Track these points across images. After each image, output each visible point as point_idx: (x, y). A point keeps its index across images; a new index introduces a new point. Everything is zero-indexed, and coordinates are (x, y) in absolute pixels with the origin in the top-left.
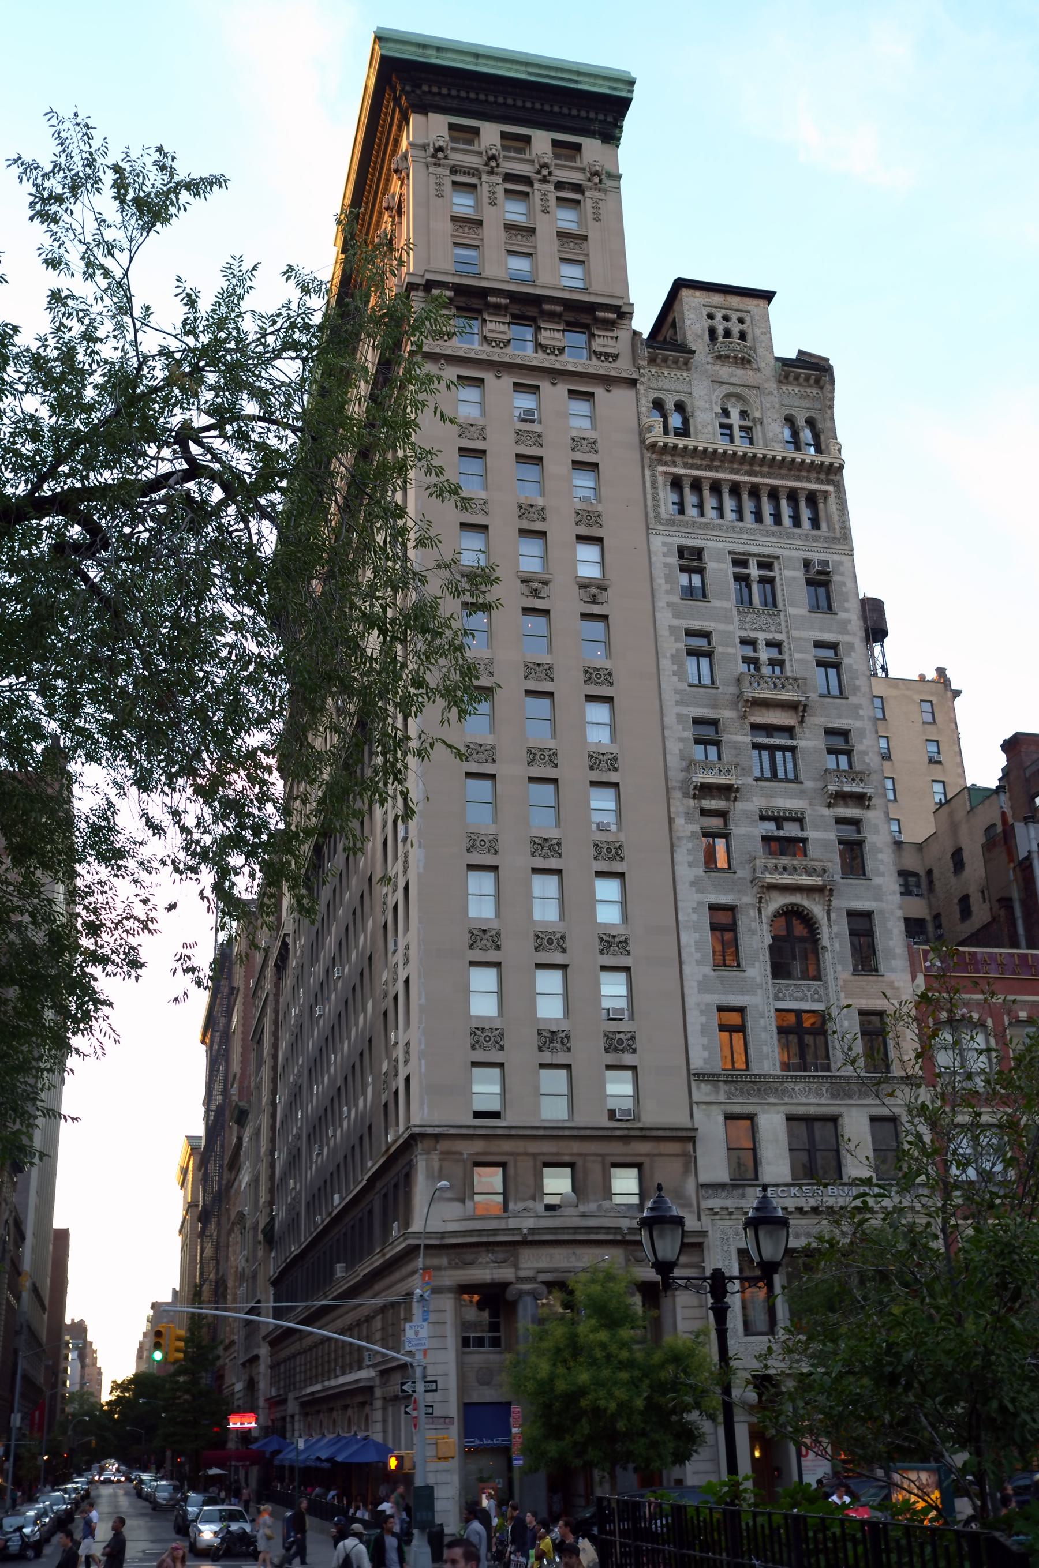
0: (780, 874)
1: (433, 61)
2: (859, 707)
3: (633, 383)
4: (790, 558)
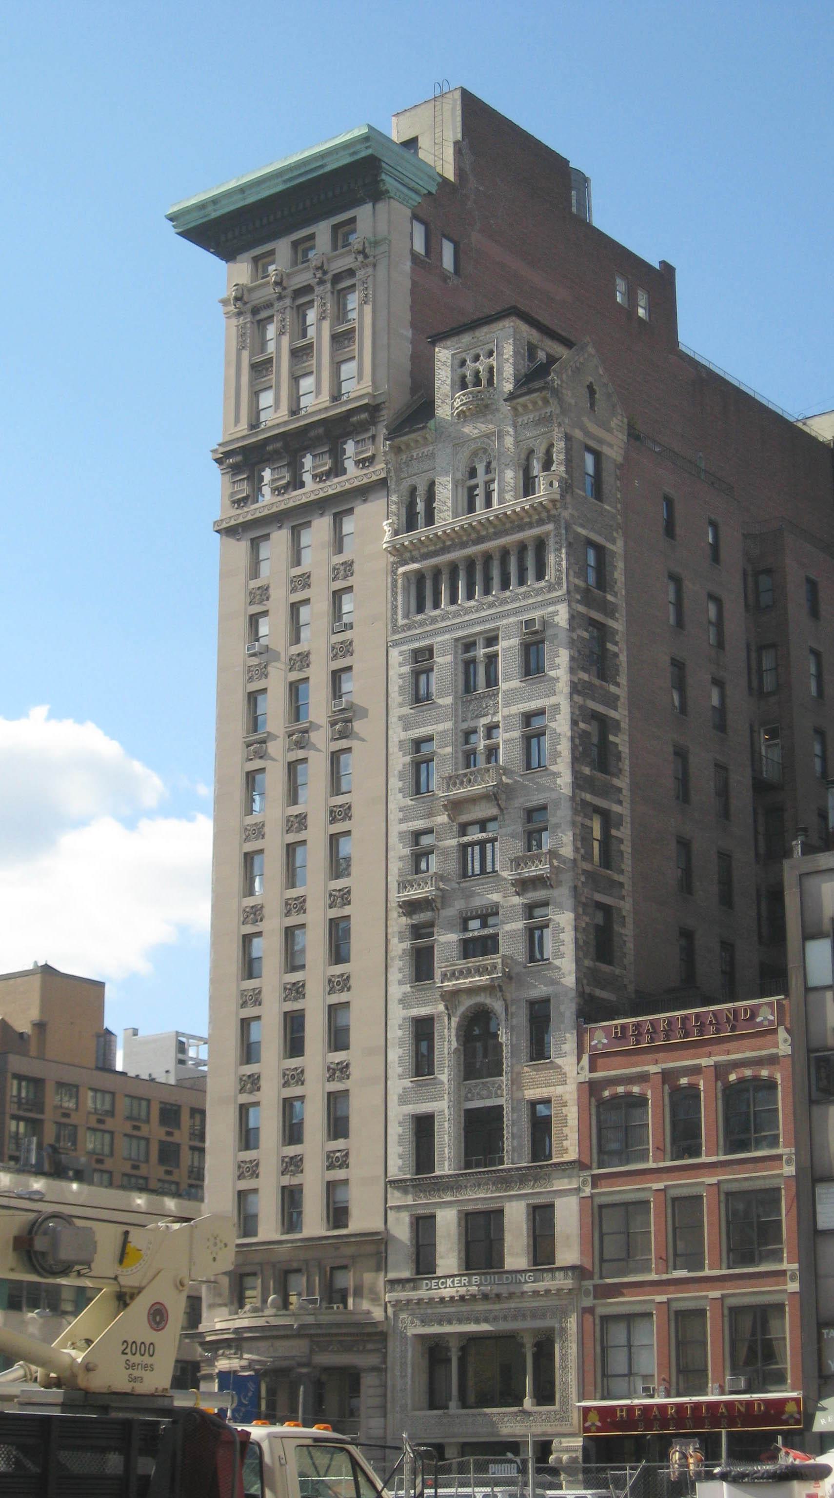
0: (457, 979)
1: (214, 215)
4: (508, 626)
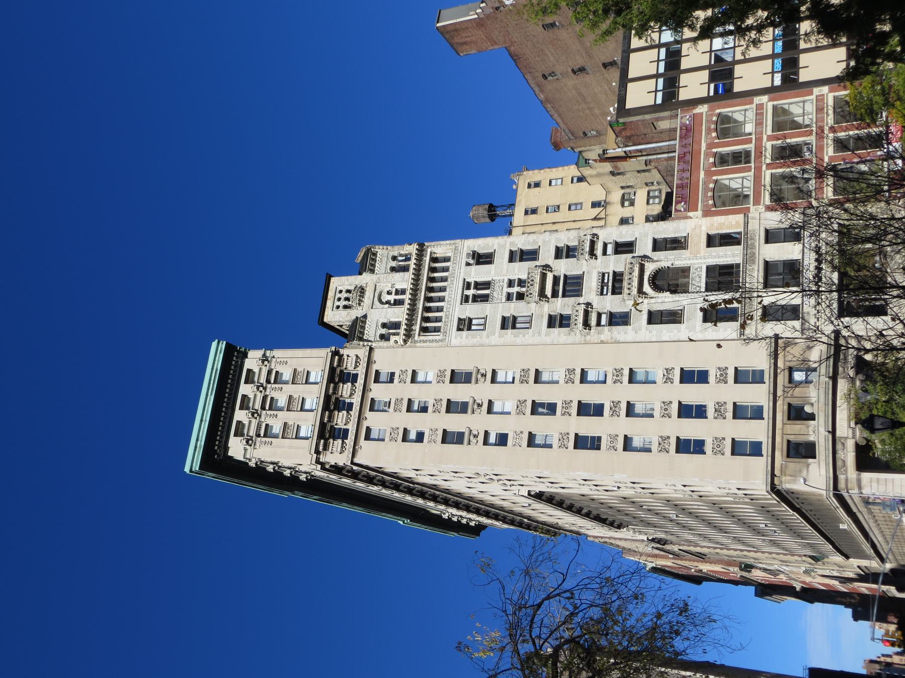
2: (544, 241)
3: (371, 349)
4: (465, 273)
